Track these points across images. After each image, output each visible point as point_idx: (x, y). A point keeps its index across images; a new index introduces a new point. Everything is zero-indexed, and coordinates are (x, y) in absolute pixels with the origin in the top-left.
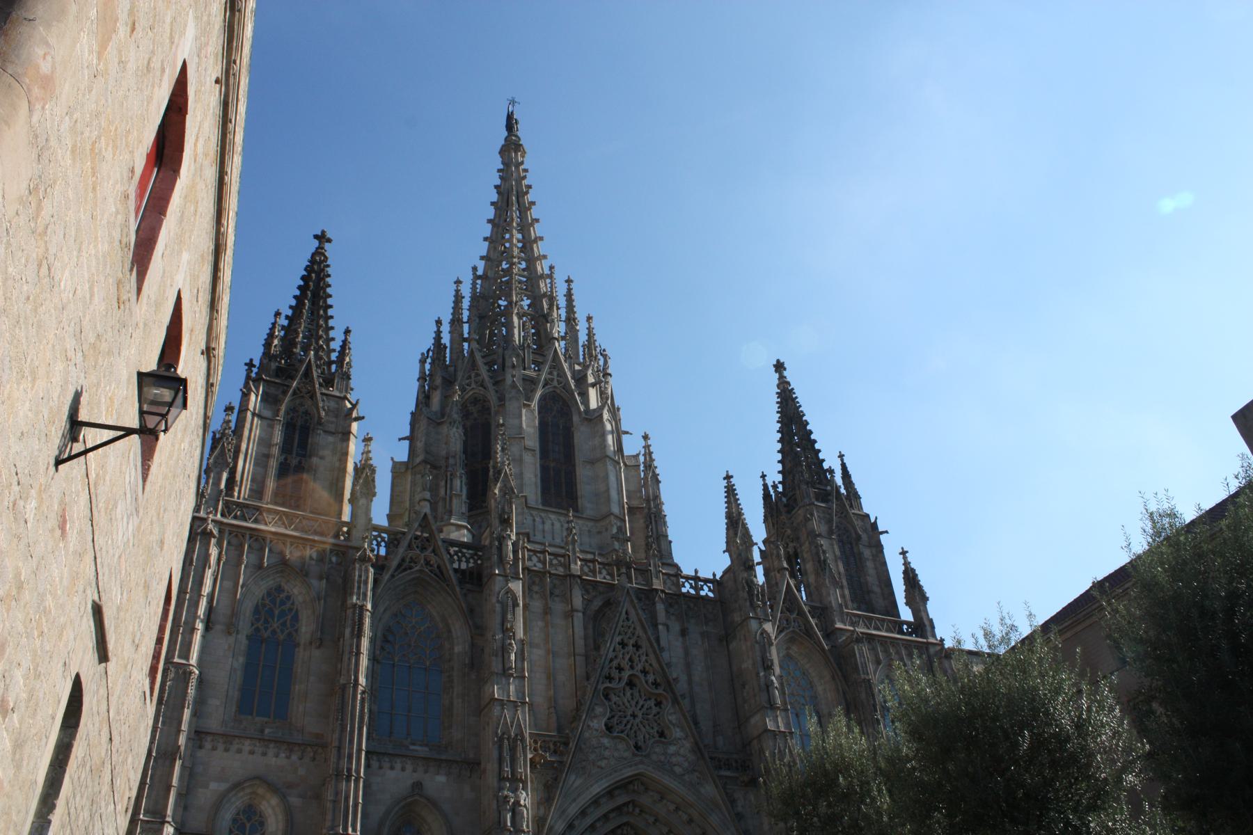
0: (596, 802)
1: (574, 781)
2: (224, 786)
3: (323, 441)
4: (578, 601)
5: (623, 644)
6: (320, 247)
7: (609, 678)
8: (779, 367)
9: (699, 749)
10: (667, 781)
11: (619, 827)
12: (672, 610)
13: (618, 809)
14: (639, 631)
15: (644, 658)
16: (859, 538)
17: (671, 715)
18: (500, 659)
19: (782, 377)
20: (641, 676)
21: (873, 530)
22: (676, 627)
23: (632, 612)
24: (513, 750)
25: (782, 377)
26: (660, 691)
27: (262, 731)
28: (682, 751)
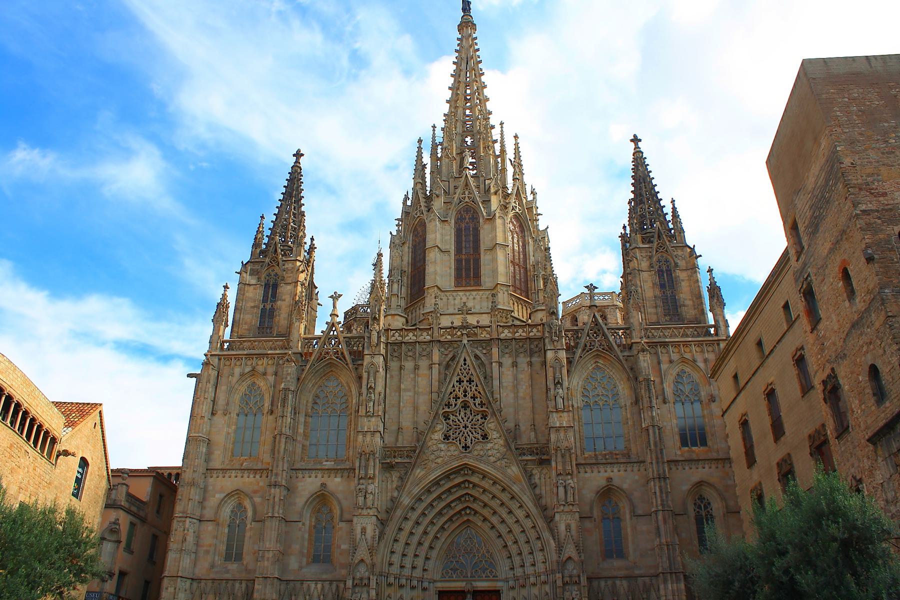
0: (437, 483)
1: (419, 472)
2: (223, 495)
3: (285, 290)
4: (436, 358)
5: (460, 381)
6: (297, 162)
7: (449, 405)
8: (636, 140)
9: (508, 444)
10: (482, 466)
11: (462, 496)
12: (507, 351)
13: (458, 485)
14: (472, 370)
15: (473, 389)
16: (676, 265)
17: (491, 425)
18: (364, 407)
19: (637, 147)
20: (471, 401)
21: (692, 254)
22: (507, 361)
23: (468, 359)
24: (368, 460)
25: (637, 147)
26: (484, 409)
27: (242, 465)
28: (496, 447)
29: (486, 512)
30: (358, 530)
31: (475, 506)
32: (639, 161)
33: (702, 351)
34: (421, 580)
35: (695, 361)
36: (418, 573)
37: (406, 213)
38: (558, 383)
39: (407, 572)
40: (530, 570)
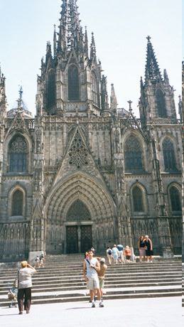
5: (76, 140)
17: (89, 158)
22: (95, 132)
25: (149, 41)
29: (86, 193)
30: (35, 201)
31: (82, 191)
32: (150, 47)
33: (175, 130)
34: (60, 221)
35: (172, 133)
36: (58, 218)
37: (44, 66)
38: (117, 141)
39: (54, 217)
40: (104, 216)
